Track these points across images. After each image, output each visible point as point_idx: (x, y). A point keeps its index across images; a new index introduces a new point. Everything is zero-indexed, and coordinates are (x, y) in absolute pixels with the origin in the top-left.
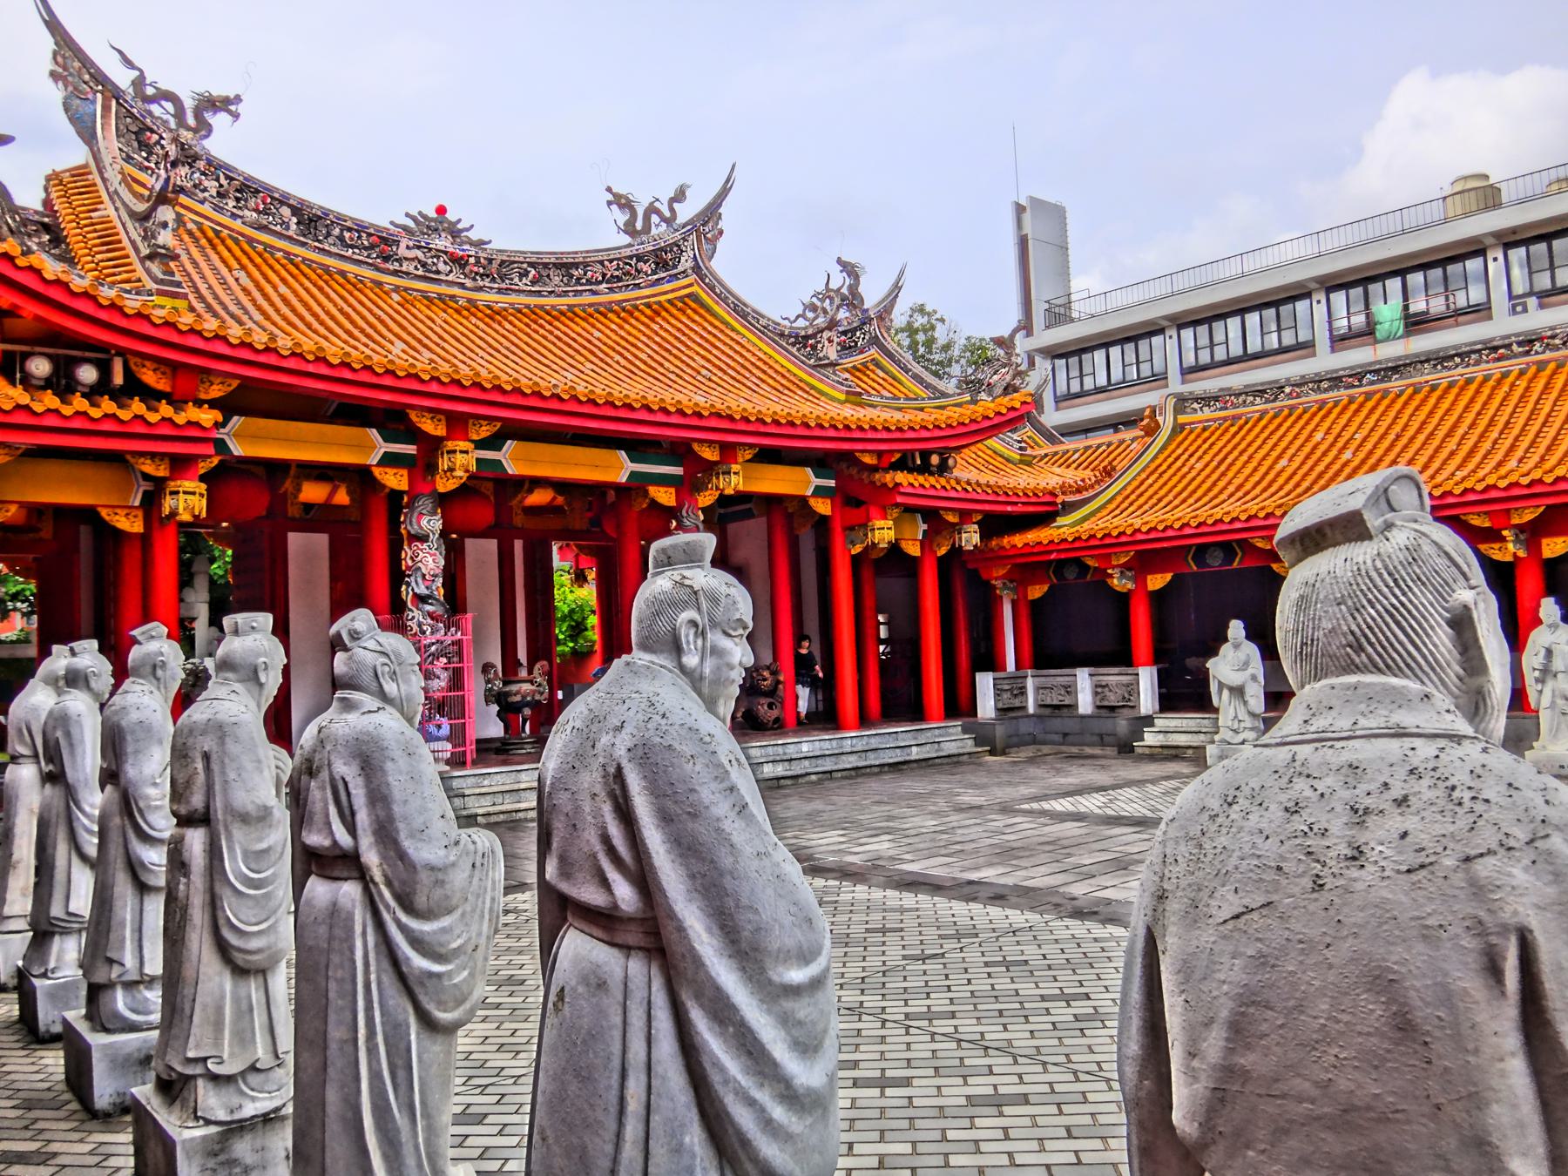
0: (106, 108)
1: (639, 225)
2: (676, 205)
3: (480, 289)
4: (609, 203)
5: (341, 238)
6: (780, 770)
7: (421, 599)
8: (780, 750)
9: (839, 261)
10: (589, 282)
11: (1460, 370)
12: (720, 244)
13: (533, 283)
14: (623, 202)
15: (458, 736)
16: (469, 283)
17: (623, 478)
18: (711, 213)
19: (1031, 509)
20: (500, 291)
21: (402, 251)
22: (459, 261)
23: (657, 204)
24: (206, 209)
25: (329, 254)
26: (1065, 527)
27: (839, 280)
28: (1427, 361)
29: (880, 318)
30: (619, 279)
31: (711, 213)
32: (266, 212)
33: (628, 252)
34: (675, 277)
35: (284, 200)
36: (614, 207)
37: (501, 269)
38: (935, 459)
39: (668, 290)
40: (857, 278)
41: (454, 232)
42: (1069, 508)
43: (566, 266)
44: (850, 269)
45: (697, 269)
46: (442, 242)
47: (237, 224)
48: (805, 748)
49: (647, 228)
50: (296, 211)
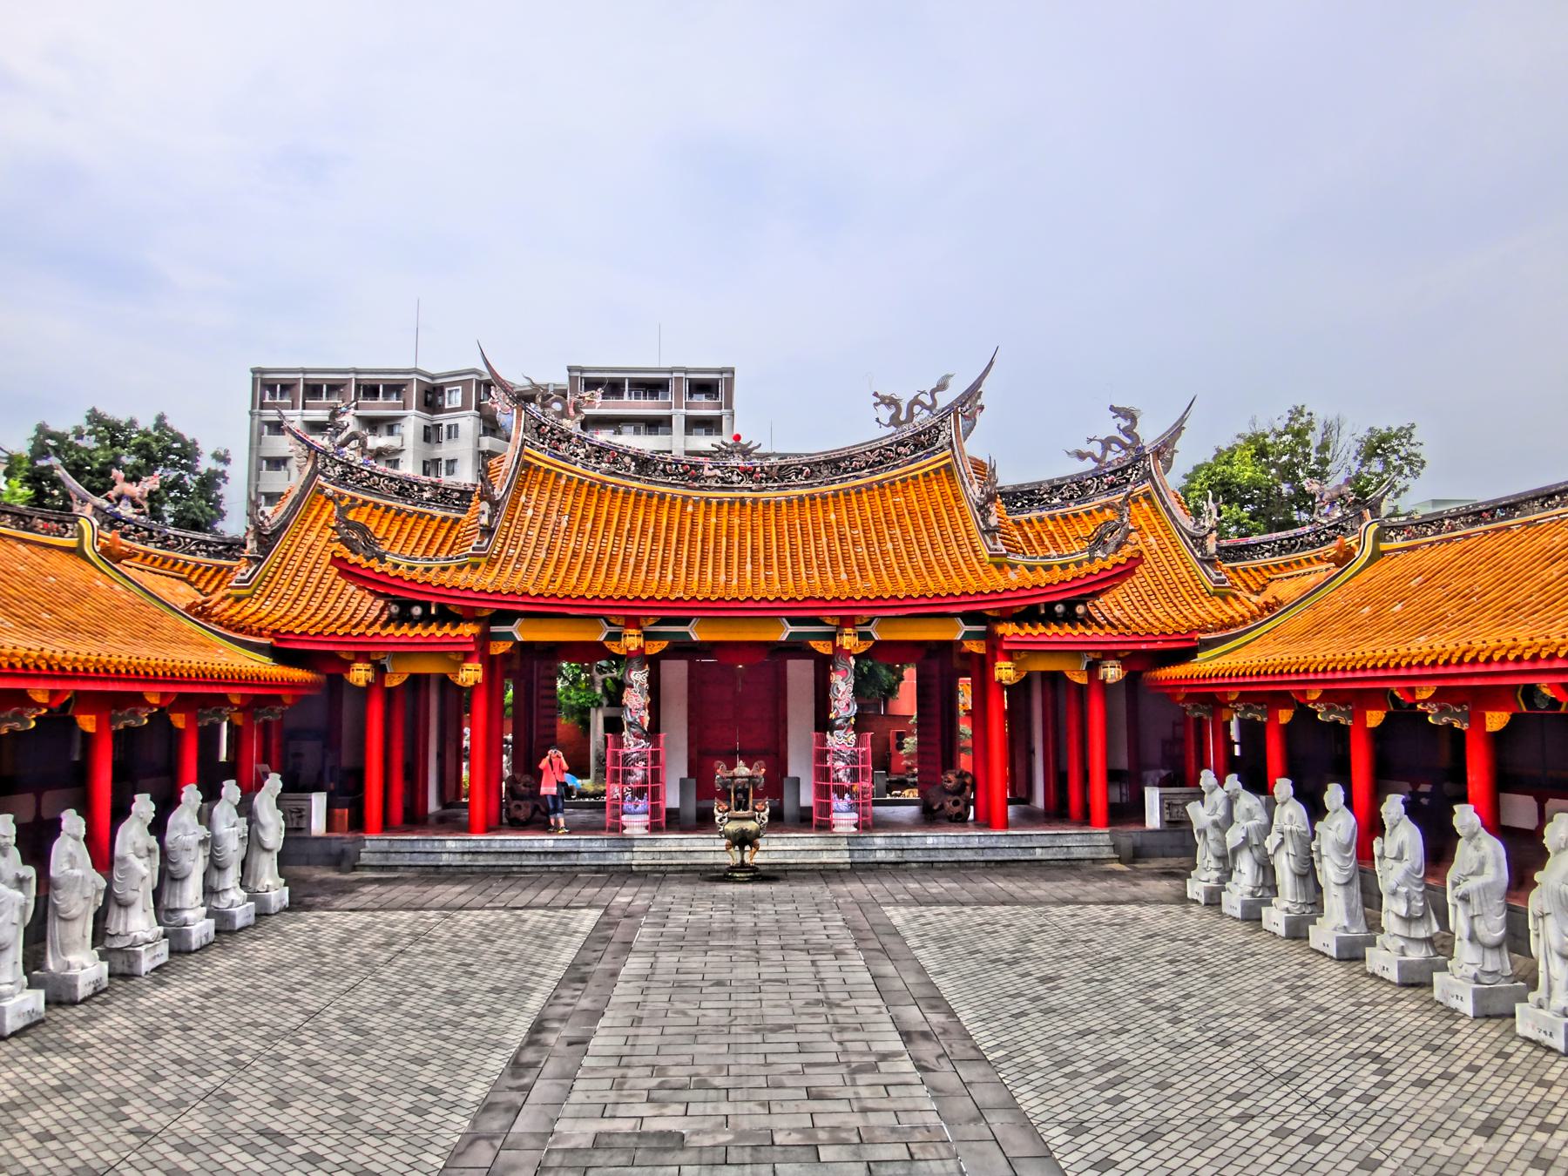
0: (519, 417)
1: (903, 417)
2: (937, 395)
3: (764, 489)
4: (876, 404)
5: (664, 471)
6: (892, 857)
7: (630, 724)
8: (904, 841)
9: (1112, 408)
10: (854, 470)
11: (1560, 510)
12: (980, 418)
13: (807, 478)
14: (891, 402)
15: (654, 812)
16: (754, 486)
17: (784, 637)
18: (973, 392)
19: (1174, 645)
20: (779, 488)
21: (707, 472)
22: (748, 473)
23: (922, 398)
24: (578, 468)
25: (656, 483)
26: (1205, 664)
27: (1111, 427)
28: (1536, 498)
29: (1158, 453)
30: (881, 463)
31: (973, 392)
32: (615, 462)
33: (888, 441)
34: (933, 453)
35: (626, 453)
36: (882, 407)
37: (781, 473)
38: (1059, 608)
39: (928, 464)
40: (1134, 419)
41: (746, 452)
42: (1208, 645)
43: (835, 464)
44: (1130, 415)
45: (951, 444)
46: (736, 461)
47: (597, 474)
48: (930, 841)
49: (911, 415)
50: (634, 458)
